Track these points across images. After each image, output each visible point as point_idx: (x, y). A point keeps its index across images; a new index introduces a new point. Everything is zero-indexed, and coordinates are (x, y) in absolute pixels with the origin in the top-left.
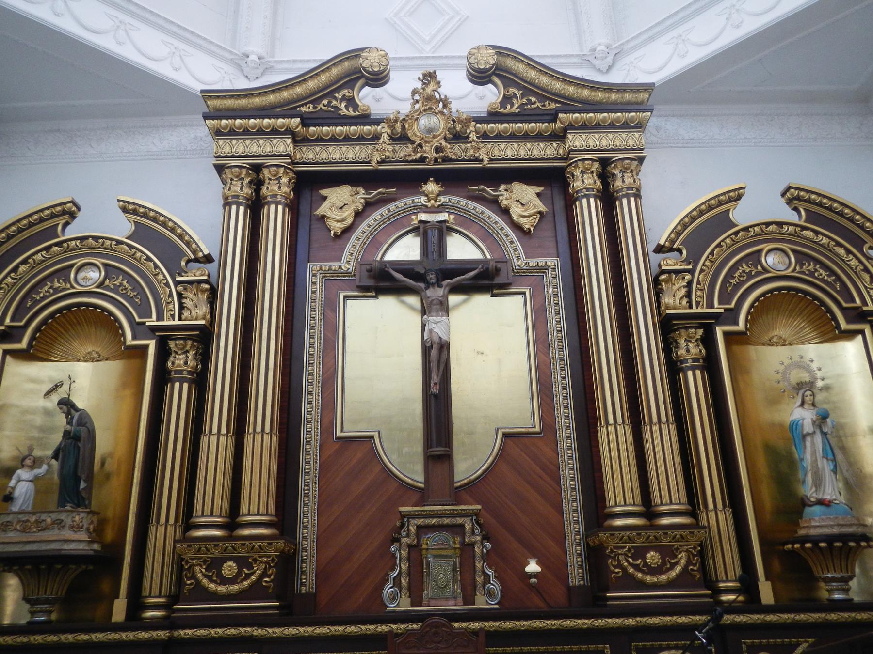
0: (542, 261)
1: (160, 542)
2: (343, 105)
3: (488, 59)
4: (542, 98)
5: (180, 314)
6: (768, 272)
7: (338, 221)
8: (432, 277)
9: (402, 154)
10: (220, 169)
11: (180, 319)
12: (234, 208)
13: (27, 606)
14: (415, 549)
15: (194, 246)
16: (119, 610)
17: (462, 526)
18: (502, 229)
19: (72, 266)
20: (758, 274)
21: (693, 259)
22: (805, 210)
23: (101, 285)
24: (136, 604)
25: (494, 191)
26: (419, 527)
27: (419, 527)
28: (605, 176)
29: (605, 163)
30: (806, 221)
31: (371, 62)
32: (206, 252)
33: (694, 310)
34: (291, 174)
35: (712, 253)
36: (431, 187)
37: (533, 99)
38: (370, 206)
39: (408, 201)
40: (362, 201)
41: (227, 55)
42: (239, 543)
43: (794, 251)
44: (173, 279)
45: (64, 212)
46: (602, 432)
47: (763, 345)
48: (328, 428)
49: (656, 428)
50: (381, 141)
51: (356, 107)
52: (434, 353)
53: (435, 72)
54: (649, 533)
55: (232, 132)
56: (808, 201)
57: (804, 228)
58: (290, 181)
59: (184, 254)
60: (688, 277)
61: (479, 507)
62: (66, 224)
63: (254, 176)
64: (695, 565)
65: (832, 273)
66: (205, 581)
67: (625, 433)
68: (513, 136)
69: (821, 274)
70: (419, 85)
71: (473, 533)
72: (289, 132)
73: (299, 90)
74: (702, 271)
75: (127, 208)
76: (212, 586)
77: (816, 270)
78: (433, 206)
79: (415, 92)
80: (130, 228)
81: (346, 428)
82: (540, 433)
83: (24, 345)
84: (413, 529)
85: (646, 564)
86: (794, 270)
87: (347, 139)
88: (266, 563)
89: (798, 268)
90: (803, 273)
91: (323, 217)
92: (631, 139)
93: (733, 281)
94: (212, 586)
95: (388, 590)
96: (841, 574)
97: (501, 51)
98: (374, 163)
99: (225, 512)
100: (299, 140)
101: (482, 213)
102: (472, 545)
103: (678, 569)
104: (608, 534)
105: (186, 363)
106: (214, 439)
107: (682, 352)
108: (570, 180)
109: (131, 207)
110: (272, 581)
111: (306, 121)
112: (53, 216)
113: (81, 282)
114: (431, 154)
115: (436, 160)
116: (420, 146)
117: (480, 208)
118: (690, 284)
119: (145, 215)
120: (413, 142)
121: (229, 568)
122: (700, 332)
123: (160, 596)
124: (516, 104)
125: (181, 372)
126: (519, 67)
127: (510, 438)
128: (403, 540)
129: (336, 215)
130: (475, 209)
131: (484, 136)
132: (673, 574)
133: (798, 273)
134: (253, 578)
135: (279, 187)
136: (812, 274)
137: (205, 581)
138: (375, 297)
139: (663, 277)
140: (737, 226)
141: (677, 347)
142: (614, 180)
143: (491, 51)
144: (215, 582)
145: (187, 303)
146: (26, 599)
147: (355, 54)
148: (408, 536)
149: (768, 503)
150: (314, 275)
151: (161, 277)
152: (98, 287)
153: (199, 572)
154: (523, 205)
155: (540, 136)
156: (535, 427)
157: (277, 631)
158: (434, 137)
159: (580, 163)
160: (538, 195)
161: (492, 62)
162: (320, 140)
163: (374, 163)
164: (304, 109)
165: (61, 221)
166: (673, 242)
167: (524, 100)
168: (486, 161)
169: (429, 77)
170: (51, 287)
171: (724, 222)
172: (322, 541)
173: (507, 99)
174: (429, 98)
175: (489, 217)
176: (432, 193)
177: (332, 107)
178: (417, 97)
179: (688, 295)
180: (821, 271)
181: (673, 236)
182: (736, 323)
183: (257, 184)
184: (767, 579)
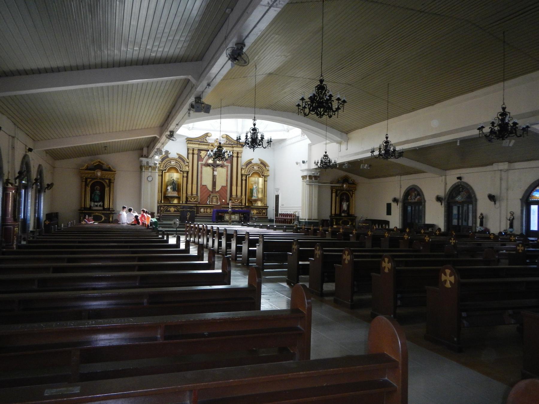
10: (188, 149)
14: (212, 198)
16: (181, 202)
21: (246, 167)
24: (182, 202)
28: (238, 154)
29: (238, 152)
31: (209, 135)
46: (233, 187)
48: (201, 184)
67: (236, 187)
72: (198, 144)
75: (177, 154)
95: (208, 202)
97: (227, 135)
100: (199, 144)
121: (193, 199)
124: (228, 142)
126: (229, 138)
127: (222, 186)
129: (202, 155)
143: (225, 136)
147: (208, 133)
149: (249, 195)
172: (201, 196)
173: (227, 142)
183: (193, 151)
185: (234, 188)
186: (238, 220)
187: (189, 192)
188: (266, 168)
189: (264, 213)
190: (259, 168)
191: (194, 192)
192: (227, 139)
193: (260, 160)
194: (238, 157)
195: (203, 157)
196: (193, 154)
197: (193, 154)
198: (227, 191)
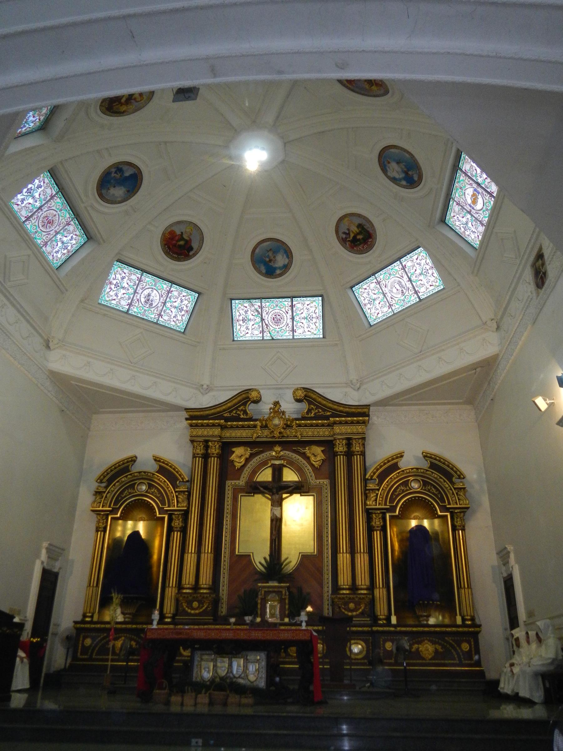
0: (321, 481)
1: (170, 594)
2: (242, 412)
3: (300, 394)
4: (324, 410)
5: (177, 505)
6: (411, 489)
7: (239, 463)
8: (275, 490)
9: (265, 434)
10: (192, 441)
11: (177, 507)
12: (197, 459)
13: (122, 616)
15: (182, 476)
17: (281, 592)
18: (306, 467)
19: (136, 483)
20: (407, 490)
21: (380, 484)
22: (430, 462)
23: (147, 492)
25: (303, 450)
26: (265, 592)
27: (265, 592)
29: (349, 439)
30: (429, 468)
31: (254, 395)
32: (187, 479)
33: (378, 507)
34: (220, 444)
35: (387, 482)
36: (278, 448)
37: (320, 410)
38: (252, 456)
39: (268, 453)
40: (249, 454)
41: (194, 386)
42: (199, 595)
43: (422, 480)
44: (174, 490)
45: (132, 461)
46: (338, 555)
47: (411, 519)
49: (359, 555)
50: (257, 429)
51: (247, 414)
52: (274, 522)
53: (279, 401)
54: (351, 596)
55: (197, 425)
56: (431, 458)
57: (427, 471)
58: (219, 446)
59: (178, 479)
60: (377, 492)
61: (288, 584)
62: (132, 466)
63: (206, 444)
64: (367, 609)
65: (437, 490)
66: (187, 609)
68: (312, 425)
69: (433, 490)
70: (272, 406)
71: (285, 595)
72: (219, 425)
73: (224, 407)
74: (383, 489)
76: (189, 611)
77: (431, 489)
78: (278, 456)
79: (270, 409)
80: (157, 467)
81: (240, 551)
82: (316, 555)
83: (118, 515)
84: (263, 592)
85: (348, 607)
86: (421, 489)
87: (243, 427)
88: (209, 603)
89: (424, 488)
90: (425, 490)
91: (233, 460)
92: (359, 428)
93: (396, 494)
94: (189, 611)
96: (426, 614)
98: (254, 438)
99: (194, 583)
100: (223, 427)
101: (298, 459)
102: (285, 599)
103: (360, 610)
104: (335, 596)
105: (179, 524)
106: (190, 555)
107: (373, 524)
108: (335, 446)
109: (158, 459)
110: (211, 609)
111: (227, 420)
112: (128, 462)
113: (139, 490)
114: (276, 434)
115: (279, 437)
116: (273, 432)
117: (298, 457)
118: (377, 494)
119: (163, 463)
120: (269, 429)
121: (195, 604)
122: (381, 515)
123: (170, 613)
125: (177, 528)
126: (314, 396)
128: (260, 597)
129: (237, 460)
130: (295, 457)
131: (299, 425)
132: (358, 613)
133: (424, 490)
134: (204, 608)
135: (215, 450)
136: (429, 491)
137: (187, 609)
138: (253, 496)
139: (367, 492)
140: (400, 469)
141: (372, 521)
142: (353, 447)
144: (190, 609)
145: (180, 500)
146: (123, 613)
148: (261, 595)
150: (229, 486)
151: (170, 489)
152: (145, 492)
153: (185, 605)
154: (315, 456)
155: (323, 425)
156: (314, 552)
157: (213, 627)
158: (279, 428)
159: (338, 441)
160: (322, 451)
161: (303, 395)
162: (232, 427)
163: (254, 438)
164: (225, 415)
165: (130, 464)
166: (372, 477)
167: (317, 411)
168: (300, 437)
169: (276, 403)
170: (128, 492)
171: (395, 467)
173: (309, 411)
174: (275, 412)
175: (301, 461)
176: (278, 451)
177: (237, 414)
178: (271, 410)
179: (376, 500)
180: (433, 489)
181: (372, 474)
182: (395, 512)
183: (207, 447)
184: (395, 615)
185: (344, 559)
186: (262, 684)
187: (188, 578)
188: (453, 483)
189: (469, 655)
190: (425, 483)
191: (206, 579)
192: (310, 403)
193: (426, 456)
194: (349, 454)
195: (238, 465)
196: (206, 457)
197: (206, 457)
198: (322, 574)
